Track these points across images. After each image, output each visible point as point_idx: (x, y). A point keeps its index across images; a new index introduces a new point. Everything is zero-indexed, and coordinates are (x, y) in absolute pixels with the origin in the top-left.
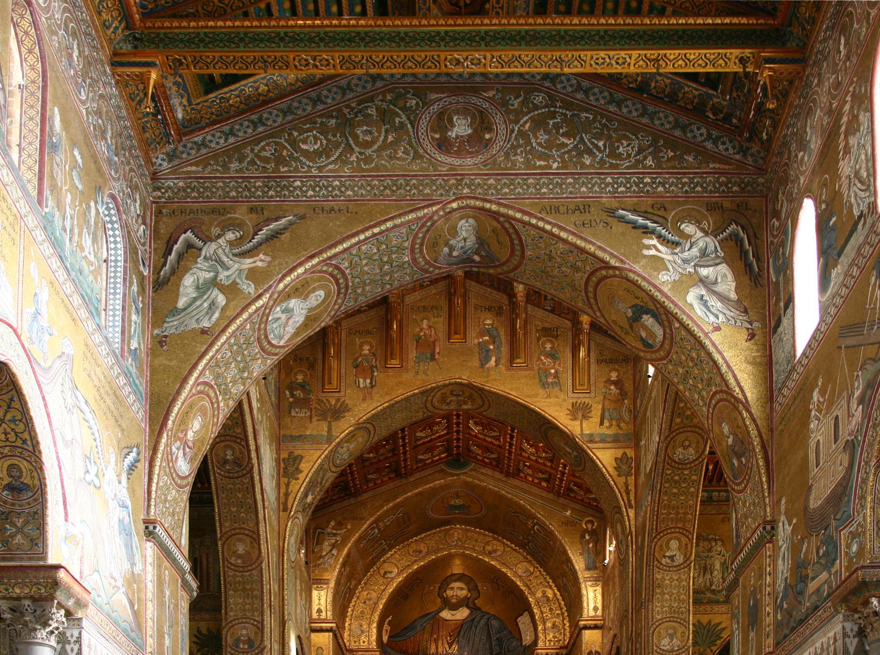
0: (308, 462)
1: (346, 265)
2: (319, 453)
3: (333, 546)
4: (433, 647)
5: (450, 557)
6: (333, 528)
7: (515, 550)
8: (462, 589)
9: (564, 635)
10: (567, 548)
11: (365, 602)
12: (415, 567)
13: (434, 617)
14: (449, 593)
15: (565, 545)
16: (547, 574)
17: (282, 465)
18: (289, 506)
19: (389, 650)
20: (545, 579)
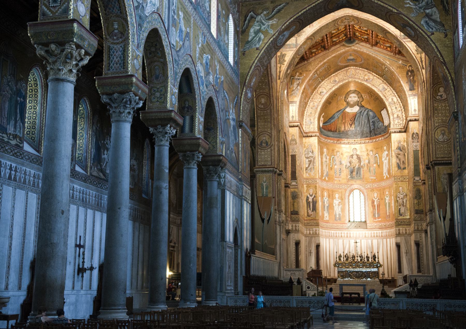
0: (288, 56)
1: (302, 17)
2: (292, 52)
3: (298, 85)
4: (343, 127)
5: (348, 83)
6: (298, 76)
7: (378, 78)
8: (355, 97)
9: (403, 121)
10: (400, 79)
11: (312, 108)
12: (334, 89)
13: (343, 112)
14: (349, 99)
15: (399, 78)
16: (394, 89)
17: (278, 59)
18: (281, 77)
19: (323, 130)
20: (393, 92)
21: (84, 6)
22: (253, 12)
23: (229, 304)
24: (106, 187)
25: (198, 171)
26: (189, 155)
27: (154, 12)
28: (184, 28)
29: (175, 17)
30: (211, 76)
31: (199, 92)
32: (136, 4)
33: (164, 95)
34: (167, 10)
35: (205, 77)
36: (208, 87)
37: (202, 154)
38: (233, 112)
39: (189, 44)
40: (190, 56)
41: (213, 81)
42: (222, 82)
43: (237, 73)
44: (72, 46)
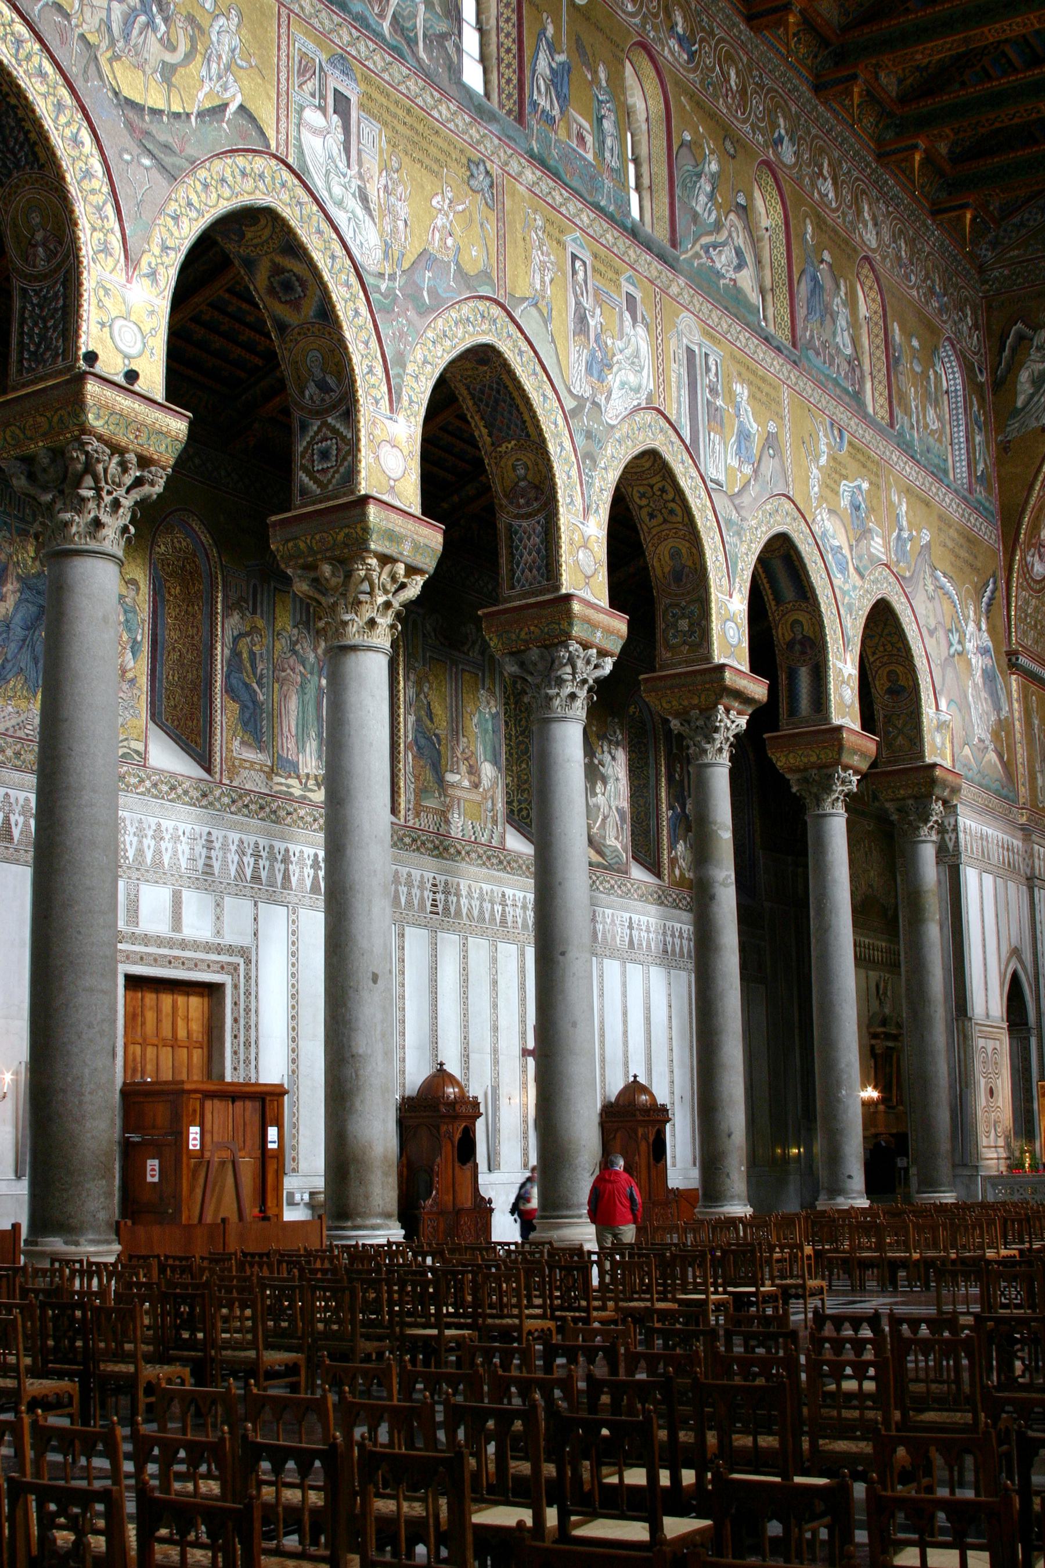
21: (399, 454)
22: (1024, 323)
23: (991, 1199)
24: (608, 886)
25: (848, 821)
26: (817, 778)
27: (637, 409)
28: (755, 425)
29: (719, 402)
30: (879, 540)
31: (831, 594)
32: (570, 404)
33: (699, 624)
34: (685, 392)
35: (851, 547)
36: (866, 574)
37: (856, 772)
38: (980, 629)
39: (778, 467)
40: (789, 498)
41: (888, 550)
42: (928, 545)
43: (985, 509)
44: (369, 561)
